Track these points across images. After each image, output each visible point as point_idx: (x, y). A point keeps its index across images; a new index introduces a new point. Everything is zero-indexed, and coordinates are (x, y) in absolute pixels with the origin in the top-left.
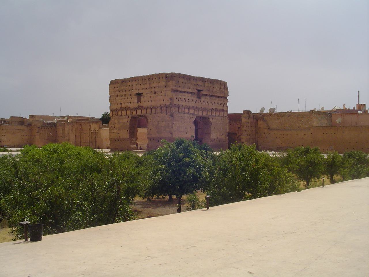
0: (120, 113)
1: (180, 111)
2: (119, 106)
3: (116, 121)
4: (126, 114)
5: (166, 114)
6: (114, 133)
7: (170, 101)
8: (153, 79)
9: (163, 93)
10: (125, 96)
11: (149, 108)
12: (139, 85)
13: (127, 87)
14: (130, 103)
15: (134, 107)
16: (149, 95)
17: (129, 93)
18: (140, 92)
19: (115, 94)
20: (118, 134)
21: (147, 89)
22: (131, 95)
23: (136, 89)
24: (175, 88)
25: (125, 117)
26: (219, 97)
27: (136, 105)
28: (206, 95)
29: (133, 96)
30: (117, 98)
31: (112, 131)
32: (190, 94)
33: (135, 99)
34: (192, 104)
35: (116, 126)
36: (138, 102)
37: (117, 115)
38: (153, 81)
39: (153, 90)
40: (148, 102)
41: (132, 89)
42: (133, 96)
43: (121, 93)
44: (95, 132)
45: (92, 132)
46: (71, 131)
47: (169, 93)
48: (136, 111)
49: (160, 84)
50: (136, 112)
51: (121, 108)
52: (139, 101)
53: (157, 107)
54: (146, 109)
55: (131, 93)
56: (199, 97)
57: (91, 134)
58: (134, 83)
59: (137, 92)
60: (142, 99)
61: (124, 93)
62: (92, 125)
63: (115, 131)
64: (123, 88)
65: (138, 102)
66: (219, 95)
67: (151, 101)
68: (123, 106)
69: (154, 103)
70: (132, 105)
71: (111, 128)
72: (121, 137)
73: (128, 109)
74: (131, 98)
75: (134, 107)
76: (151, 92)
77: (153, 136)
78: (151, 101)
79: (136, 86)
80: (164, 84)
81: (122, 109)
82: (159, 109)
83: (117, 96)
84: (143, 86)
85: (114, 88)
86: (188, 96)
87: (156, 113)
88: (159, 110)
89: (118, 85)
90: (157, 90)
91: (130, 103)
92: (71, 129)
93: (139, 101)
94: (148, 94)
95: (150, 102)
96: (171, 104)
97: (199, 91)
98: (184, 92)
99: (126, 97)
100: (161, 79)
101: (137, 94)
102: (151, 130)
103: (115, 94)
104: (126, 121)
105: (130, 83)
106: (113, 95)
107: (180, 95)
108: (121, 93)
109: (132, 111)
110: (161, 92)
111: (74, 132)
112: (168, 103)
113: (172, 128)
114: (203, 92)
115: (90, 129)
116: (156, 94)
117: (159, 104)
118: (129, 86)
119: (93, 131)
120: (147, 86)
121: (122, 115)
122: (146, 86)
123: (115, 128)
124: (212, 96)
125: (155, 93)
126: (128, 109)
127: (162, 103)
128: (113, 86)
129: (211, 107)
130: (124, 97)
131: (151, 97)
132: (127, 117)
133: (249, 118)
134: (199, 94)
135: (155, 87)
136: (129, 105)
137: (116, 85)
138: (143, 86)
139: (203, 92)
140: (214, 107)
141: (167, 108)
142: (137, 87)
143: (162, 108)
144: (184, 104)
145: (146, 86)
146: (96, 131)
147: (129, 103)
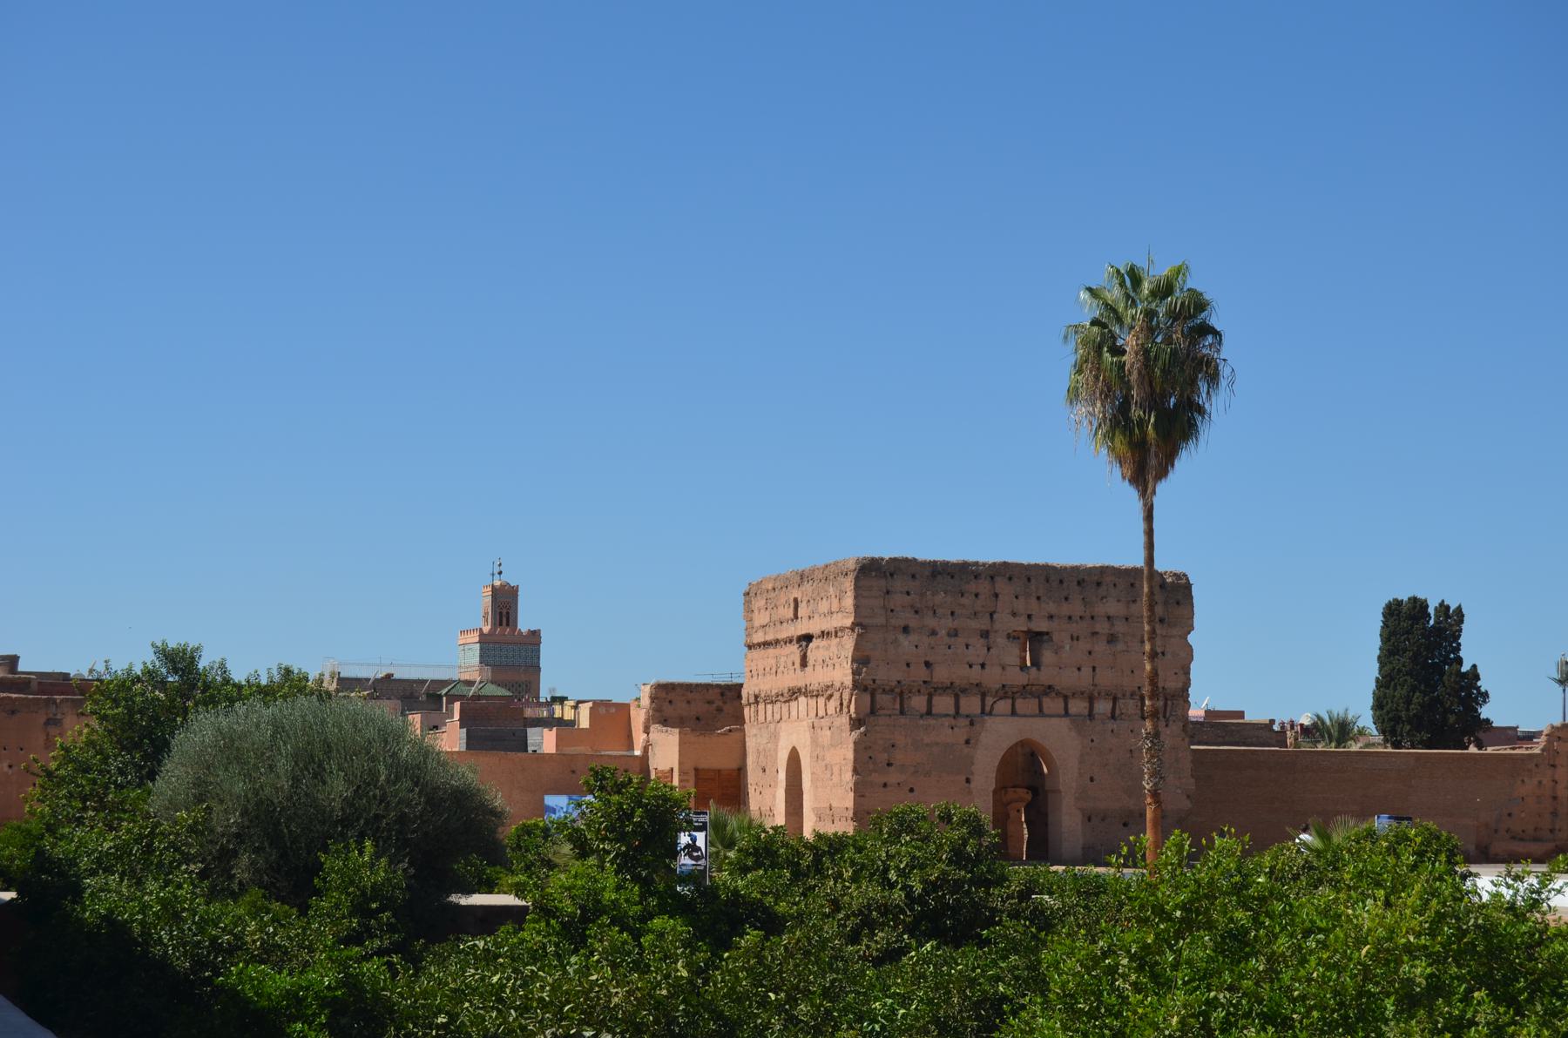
0: (918, 702)
2: (920, 673)
4: (952, 711)
5: (1167, 726)
6: (885, 785)
8: (1099, 584)
10: (954, 633)
11: (1082, 693)
12: (1034, 600)
13: (964, 601)
14: (983, 666)
15: (1004, 686)
16: (1084, 645)
17: (975, 624)
18: (1041, 625)
19: (893, 621)
20: (911, 790)
21: (1070, 618)
22: (985, 634)
23: (1014, 614)
25: (953, 722)
27: (1017, 678)
29: (1001, 640)
30: (906, 642)
31: (878, 779)
37: (902, 712)
39: (1103, 627)
40: (1079, 669)
41: (994, 612)
42: (1001, 640)
43: (931, 622)
48: (1010, 701)
50: (1010, 707)
51: (925, 682)
53: (1124, 695)
54: (1066, 698)
55: (989, 628)
58: (1001, 585)
59: (1021, 625)
60: (1047, 656)
61: (949, 623)
63: (893, 777)
67: (1094, 669)
68: (941, 674)
69: (1106, 678)
70: (992, 678)
71: (871, 767)
73: (964, 691)
74: (988, 649)
75: (1004, 686)
76: (1094, 634)
78: (1094, 669)
79: (1015, 599)
81: (932, 690)
83: (906, 630)
84: (1051, 607)
85: (888, 592)
87: (1113, 717)
90: (1120, 627)
91: (983, 666)
94: (1078, 639)
95: (1086, 671)
99: (961, 641)
102: (1092, 780)
103: (893, 621)
104: (962, 741)
105: (983, 587)
106: (881, 620)
108: (931, 622)
109: (989, 701)
116: (1120, 646)
118: (977, 595)
120: (1076, 607)
121: (929, 713)
122: (1066, 609)
123: (889, 765)
125: (1112, 639)
126: (964, 691)
130: (947, 640)
131: (1090, 653)
135: (1109, 618)
136: (975, 674)
137: (898, 584)
138: (1051, 607)
141: (1166, 699)
142: (1020, 605)
145: (1066, 609)
147: (977, 668)
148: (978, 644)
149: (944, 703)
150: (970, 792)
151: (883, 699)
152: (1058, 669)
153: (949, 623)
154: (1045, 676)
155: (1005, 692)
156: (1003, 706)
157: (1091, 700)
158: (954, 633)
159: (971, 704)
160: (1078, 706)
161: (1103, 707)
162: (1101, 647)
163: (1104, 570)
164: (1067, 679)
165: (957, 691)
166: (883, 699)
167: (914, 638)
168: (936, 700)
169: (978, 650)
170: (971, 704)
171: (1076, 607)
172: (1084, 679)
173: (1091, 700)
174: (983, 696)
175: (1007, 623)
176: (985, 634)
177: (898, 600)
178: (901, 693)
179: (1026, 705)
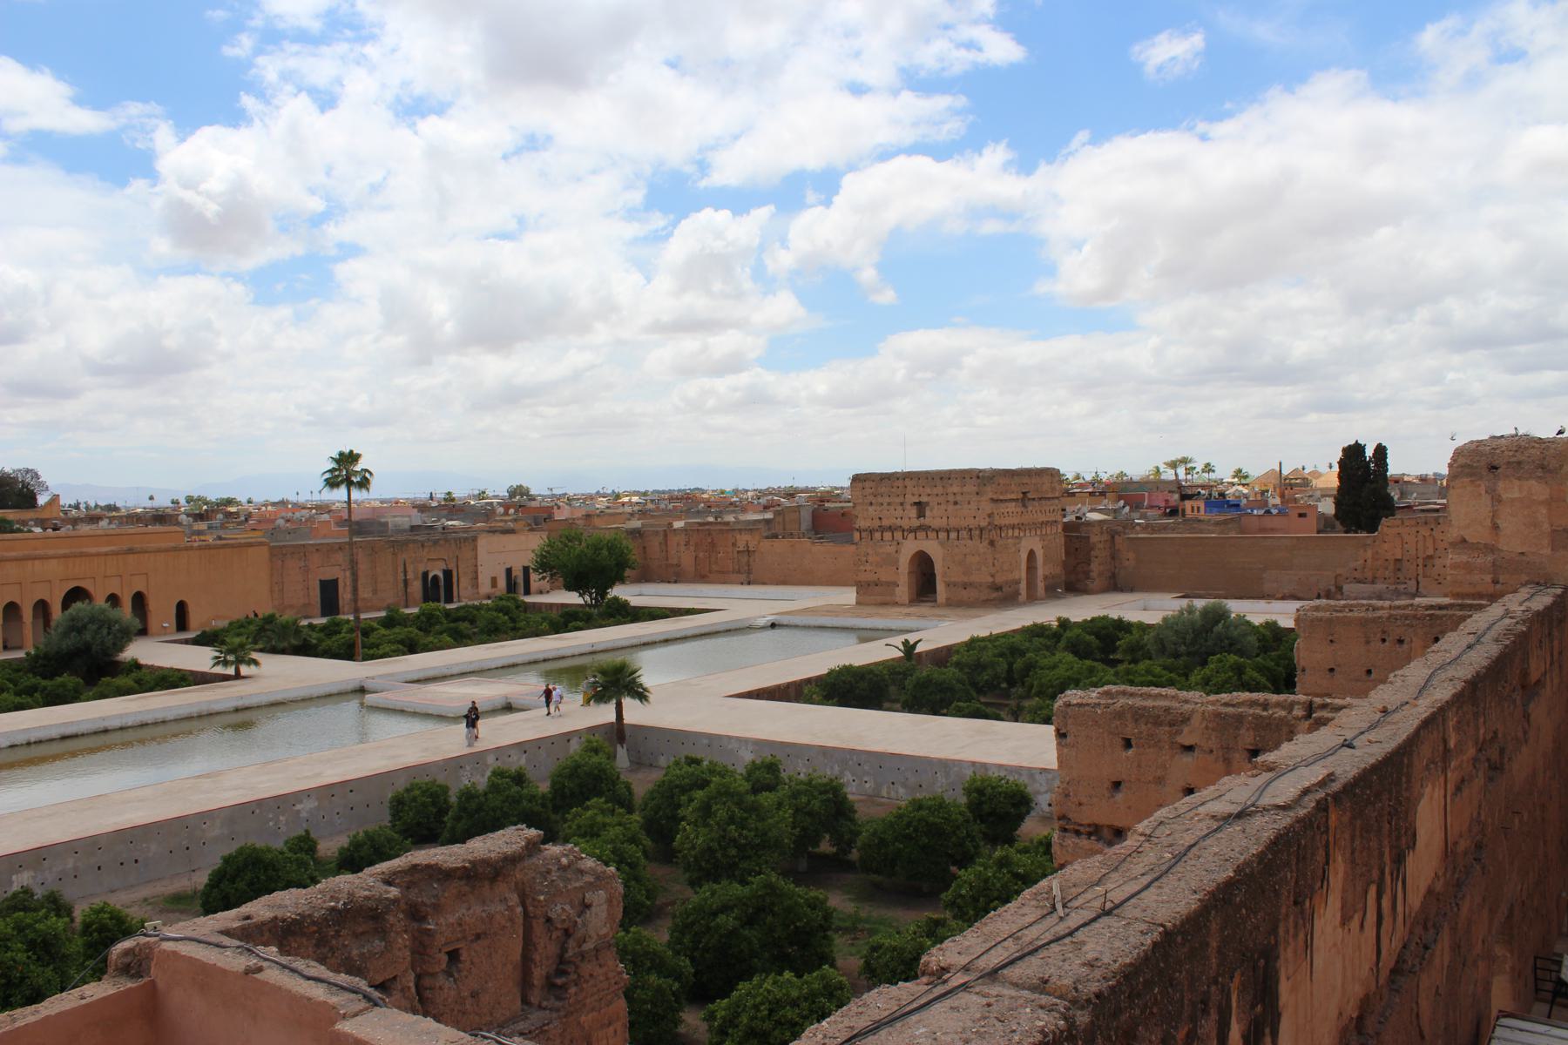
0: (877, 535)
1: (1003, 535)
2: (877, 523)
3: (870, 551)
7: (987, 520)
9: (973, 506)
10: (889, 504)
16: (943, 507)
17: (900, 499)
18: (924, 499)
22: (902, 504)
23: (913, 495)
24: (995, 497)
26: (1049, 499)
27: (916, 523)
28: (1034, 499)
29: (908, 507)
30: (870, 509)
31: (862, 567)
32: (1014, 504)
33: (913, 512)
34: (1015, 521)
35: (870, 559)
36: (919, 517)
38: (950, 481)
39: (951, 498)
42: (908, 507)
44: (749, 551)
45: (738, 552)
46: (683, 548)
47: (987, 507)
49: (965, 489)
52: (921, 514)
56: (1024, 506)
57: (735, 553)
58: (908, 482)
60: (928, 513)
61: (887, 500)
62: (738, 537)
63: (868, 567)
64: (883, 489)
65: (919, 517)
66: (1050, 495)
68: (886, 523)
69: (953, 522)
70: (905, 524)
72: (883, 579)
77: (953, 580)
80: (975, 489)
81: (882, 529)
82: (965, 533)
83: (871, 504)
84: (928, 491)
86: (1012, 507)
88: (964, 534)
89: (872, 484)
90: (959, 498)
92: (683, 543)
93: (921, 514)
95: (945, 519)
96: (989, 524)
97: (1024, 493)
98: (1006, 500)
99: (892, 508)
100: (968, 479)
101: (915, 503)
105: (900, 483)
106: (861, 501)
107: (1003, 508)
108: (880, 500)
109: (906, 534)
110: (969, 503)
111: (692, 548)
112: (984, 524)
113: (994, 565)
114: (1030, 496)
115: (734, 545)
116: (958, 507)
117: (963, 523)
119: (741, 549)
120: (939, 490)
122: (935, 491)
124: (1040, 499)
125: (956, 503)
127: (972, 523)
128: (860, 485)
129: (1040, 520)
132: (895, 543)
133: (1102, 533)
134: (1024, 499)
136: (899, 522)
137: (867, 484)
138: (928, 491)
139: (1030, 496)
140: (1045, 519)
143: (971, 530)
144: (1007, 521)
145: (935, 491)
146: (751, 549)
148: (899, 508)
149: (887, 535)
150: (898, 574)
151: (864, 534)
152: (934, 517)
153: (887, 500)
154: (927, 521)
155: (911, 530)
156: (912, 535)
157: (948, 532)
158: (889, 504)
159: (898, 535)
160: (942, 535)
161: (953, 535)
162: (951, 507)
163: (951, 472)
164: (936, 523)
165: (891, 529)
166: (864, 534)
167: (874, 507)
168: (885, 534)
169: (899, 512)
170: (898, 535)
171: (939, 490)
172: (942, 523)
173: (948, 532)
174: (903, 531)
175: (911, 499)
176: (902, 504)
177: (868, 491)
178: (871, 532)
179: (921, 535)
